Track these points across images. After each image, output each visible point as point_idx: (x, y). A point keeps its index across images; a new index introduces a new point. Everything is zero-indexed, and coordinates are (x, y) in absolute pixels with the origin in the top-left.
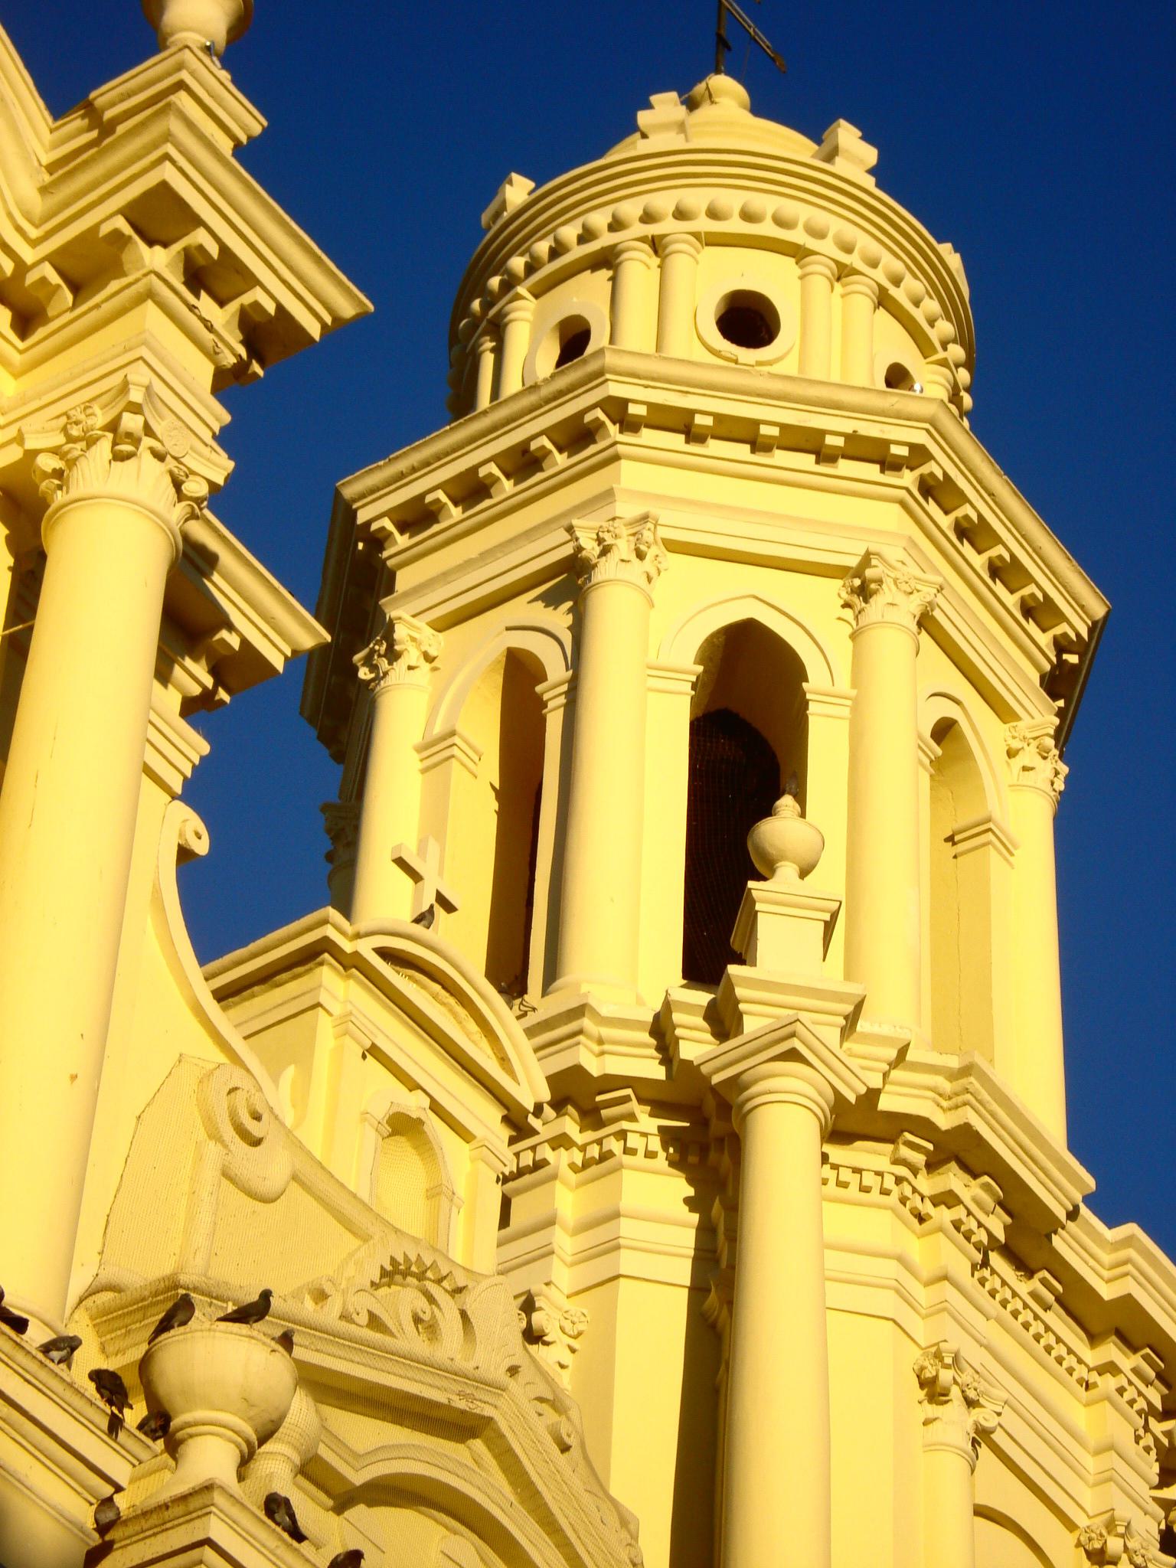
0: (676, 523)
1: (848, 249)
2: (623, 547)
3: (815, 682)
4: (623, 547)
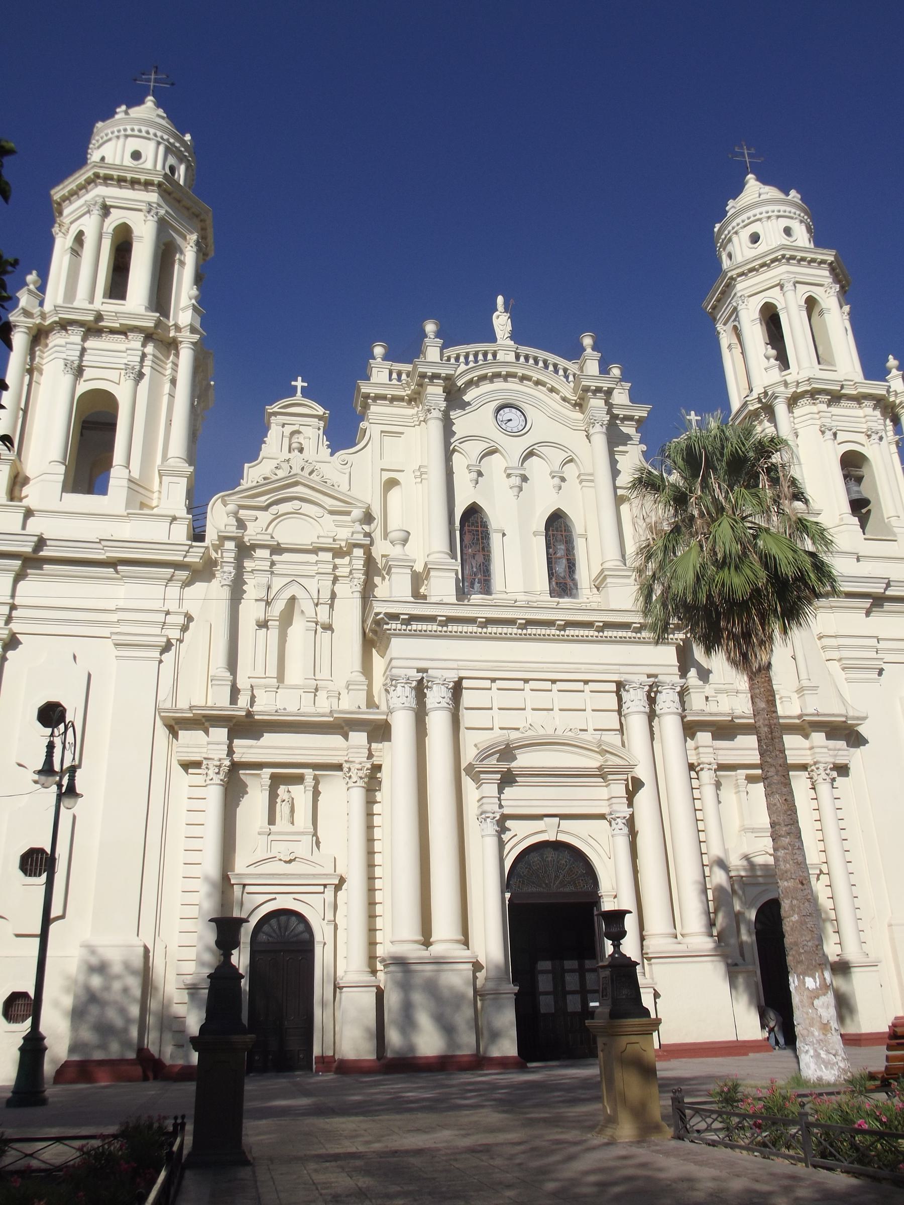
0: (747, 293)
1: (767, 212)
2: (740, 302)
3: (779, 307)
4: (740, 302)
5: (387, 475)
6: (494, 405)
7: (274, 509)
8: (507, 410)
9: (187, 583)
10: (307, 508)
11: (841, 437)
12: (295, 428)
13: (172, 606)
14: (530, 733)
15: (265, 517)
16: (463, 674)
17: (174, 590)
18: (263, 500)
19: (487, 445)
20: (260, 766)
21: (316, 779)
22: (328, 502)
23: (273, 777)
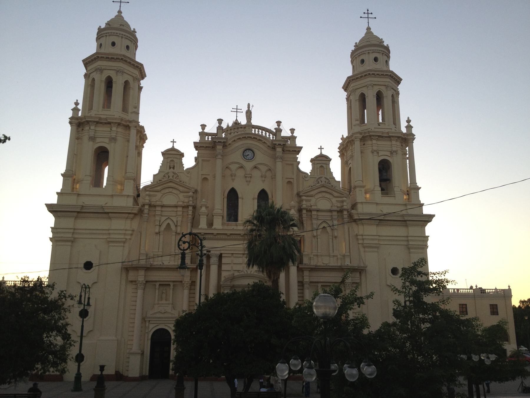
6: (242, 149)
7: (163, 192)
8: (247, 151)
9: (132, 219)
10: (174, 191)
11: (381, 153)
12: (172, 159)
14: (242, 273)
15: (159, 195)
16: (222, 252)
17: (129, 221)
18: (159, 188)
19: (239, 165)
20: (156, 281)
21: (174, 285)
22: (181, 189)
23: (160, 285)
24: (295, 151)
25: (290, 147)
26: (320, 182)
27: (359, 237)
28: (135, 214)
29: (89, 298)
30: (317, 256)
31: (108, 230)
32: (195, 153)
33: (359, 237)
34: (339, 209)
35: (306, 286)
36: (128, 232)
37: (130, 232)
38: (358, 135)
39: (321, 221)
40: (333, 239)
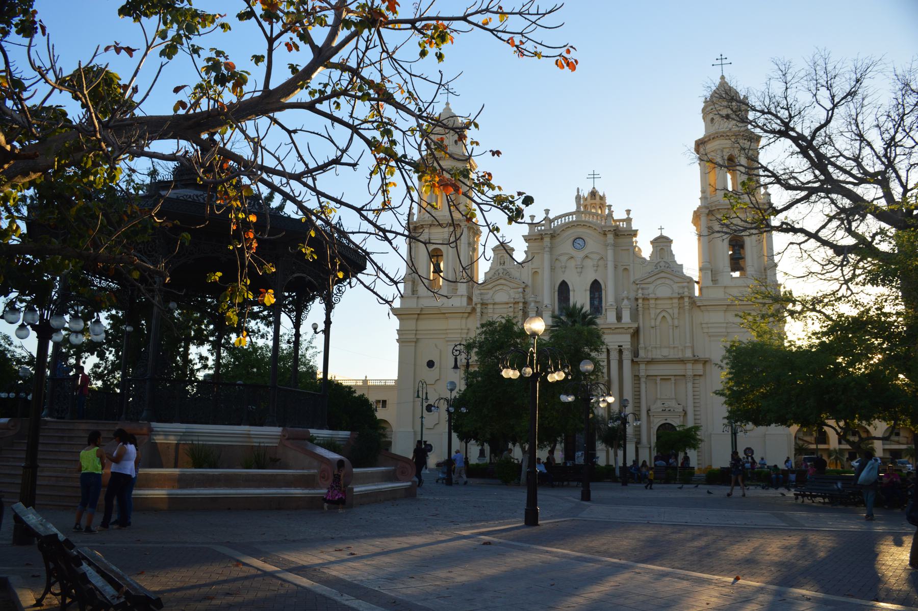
5: (534, 270)
7: (494, 289)
9: (467, 318)
10: (505, 288)
12: (502, 255)
13: (463, 327)
15: (491, 292)
17: (464, 321)
24: (631, 234)
25: (626, 231)
26: (659, 267)
27: (704, 326)
28: (469, 313)
29: (427, 393)
30: (656, 348)
31: (446, 330)
32: (524, 246)
33: (704, 326)
34: (679, 296)
35: (643, 380)
36: (464, 331)
37: (466, 331)
38: (704, 210)
39: (659, 311)
40: (673, 329)
